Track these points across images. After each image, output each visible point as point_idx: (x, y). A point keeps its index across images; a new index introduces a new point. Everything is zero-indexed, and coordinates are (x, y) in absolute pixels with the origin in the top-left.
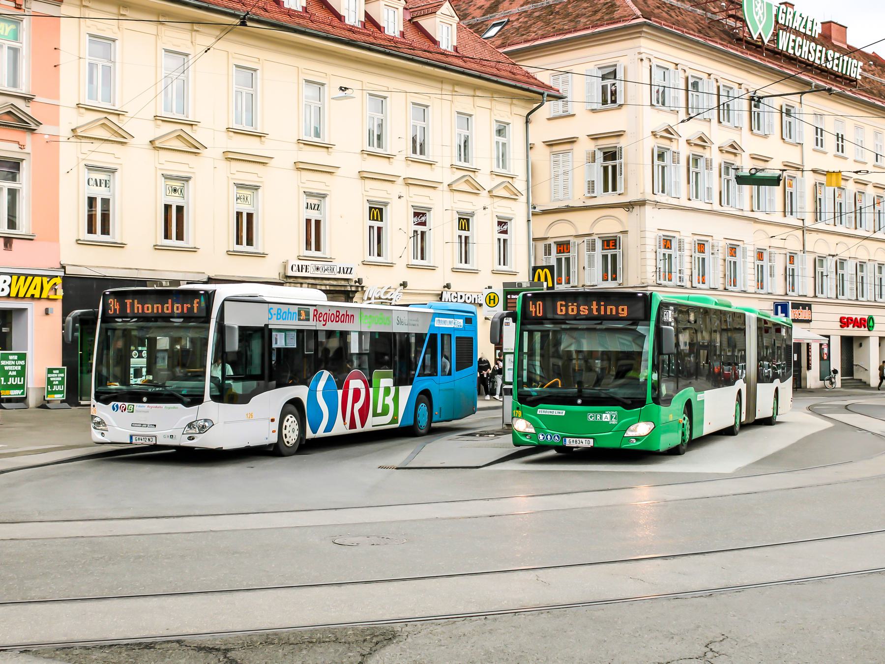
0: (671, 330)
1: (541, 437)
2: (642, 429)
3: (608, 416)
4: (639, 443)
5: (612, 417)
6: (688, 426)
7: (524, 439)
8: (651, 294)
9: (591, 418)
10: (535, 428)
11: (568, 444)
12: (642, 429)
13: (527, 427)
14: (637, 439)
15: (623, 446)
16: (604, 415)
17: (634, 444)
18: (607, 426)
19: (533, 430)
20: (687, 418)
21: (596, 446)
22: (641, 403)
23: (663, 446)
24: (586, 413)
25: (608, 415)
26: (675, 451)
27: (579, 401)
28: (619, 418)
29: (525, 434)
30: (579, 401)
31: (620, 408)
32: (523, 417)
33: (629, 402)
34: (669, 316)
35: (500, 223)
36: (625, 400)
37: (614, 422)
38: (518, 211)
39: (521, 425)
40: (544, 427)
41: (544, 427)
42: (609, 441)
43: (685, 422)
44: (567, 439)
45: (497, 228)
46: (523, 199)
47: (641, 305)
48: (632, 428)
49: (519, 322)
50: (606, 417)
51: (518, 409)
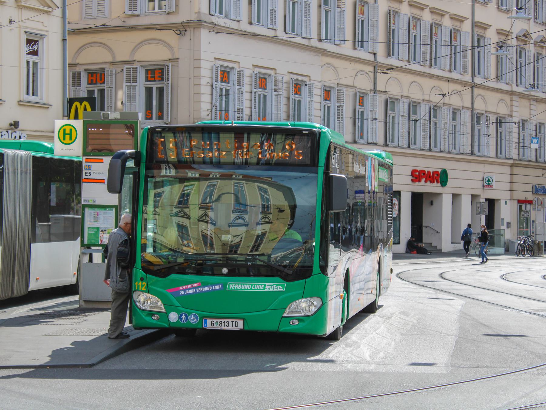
7: (148, 319)
11: (209, 326)
15: (282, 329)
17: (295, 326)
21: (247, 328)
27: (225, 271)
29: (151, 314)
32: (148, 291)
35: (29, 42)
38: (51, 27)
40: (177, 304)
41: (177, 304)
44: (209, 321)
45: (25, 48)
46: (58, 12)
51: (142, 279)
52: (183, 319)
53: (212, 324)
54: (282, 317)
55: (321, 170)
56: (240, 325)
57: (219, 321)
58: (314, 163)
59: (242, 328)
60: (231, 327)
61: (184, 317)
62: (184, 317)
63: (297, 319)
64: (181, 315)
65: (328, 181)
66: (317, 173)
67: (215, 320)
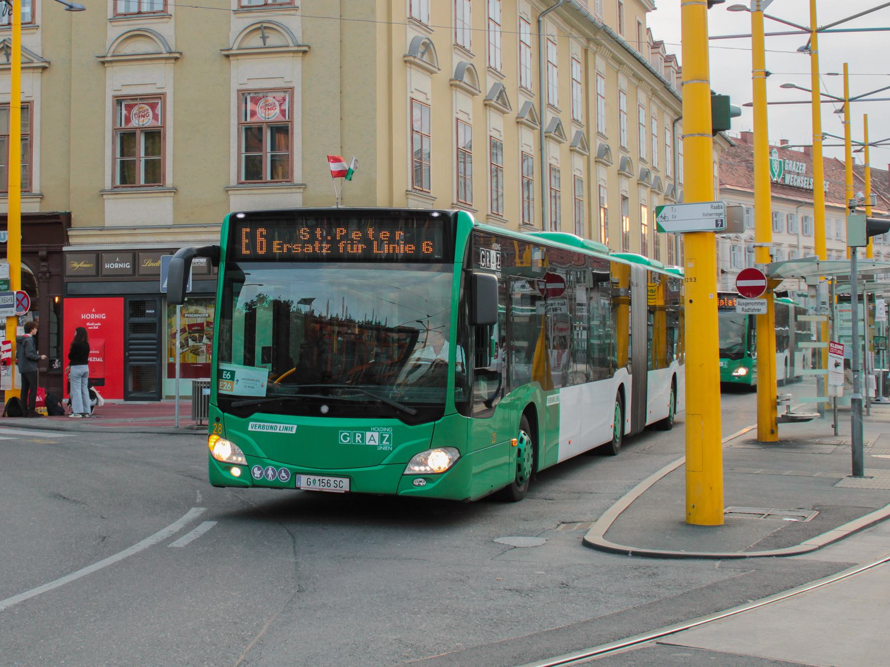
0: (492, 280)
1: (257, 473)
2: (438, 460)
3: (376, 435)
4: (431, 486)
5: (382, 438)
6: (528, 452)
8: (456, 214)
9: (344, 439)
10: (246, 455)
12: (438, 460)
13: (234, 453)
14: (428, 477)
16: (368, 434)
17: (421, 487)
18: (372, 455)
19: (241, 459)
20: (526, 438)
21: (354, 490)
22: (434, 412)
23: (475, 490)
24: (335, 431)
25: (375, 434)
26: (505, 496)
27: (325, 409)
28: (396, 440)
30: (325, 409)
31: (396, 422)
33: (413, 412)
34: (492, 257)
36: (407, 409)
37: (386, 446)
39: (222, 449)
40: (261, 454)
41: (261, 454)
42: (377, 481)
43: (523, 446)
47: (438, 235)
48: (419, 458)
49: (222, 266)
50: (372, 438)
51: (218, 420)
52: (270, 476)
53: (309, 483)
54: (403, 475)
55: (458, 266)
56: (344, 485)
57: (317, 478)
58: (448, 258)
59: (348, 489)
60: (332, 489)
61: (270, 472)
62: (270, 472)
63: (424, 478)
64: (268, 469)
65: (470, 283)
66: (451, 271)
67: (312, 478)
